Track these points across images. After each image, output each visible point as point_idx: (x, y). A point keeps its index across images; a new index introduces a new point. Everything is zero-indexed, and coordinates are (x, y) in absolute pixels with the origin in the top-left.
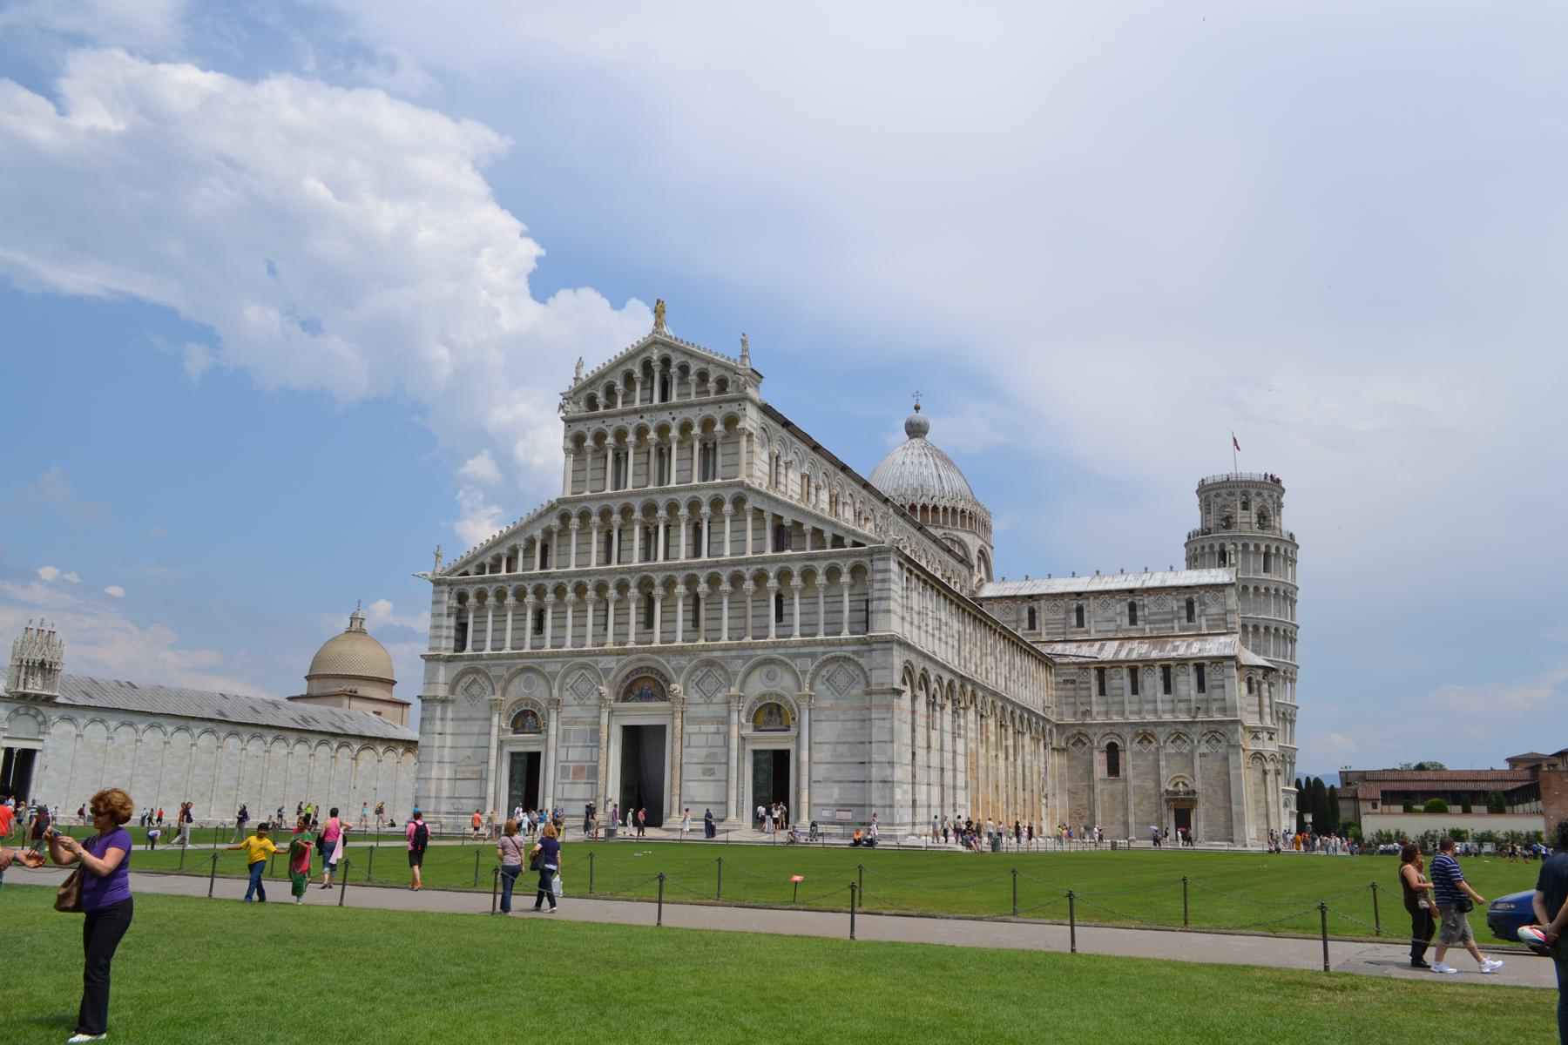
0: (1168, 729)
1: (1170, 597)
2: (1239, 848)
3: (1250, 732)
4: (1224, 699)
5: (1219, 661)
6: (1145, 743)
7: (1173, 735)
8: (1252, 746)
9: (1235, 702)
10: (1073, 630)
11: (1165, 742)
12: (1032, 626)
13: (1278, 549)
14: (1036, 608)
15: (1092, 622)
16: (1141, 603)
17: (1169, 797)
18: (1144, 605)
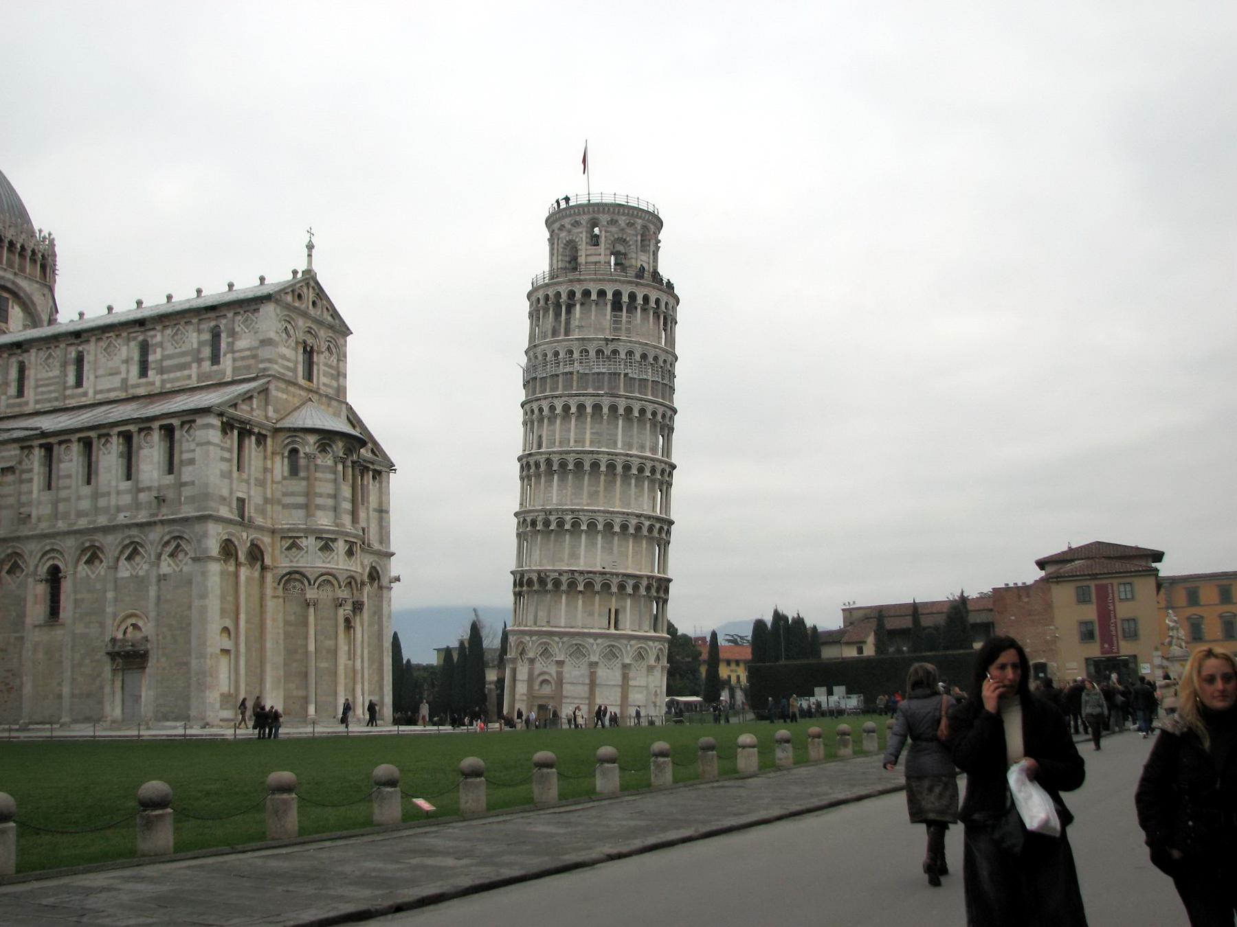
0: (119, 536)
1: (190, 328)
2: (195, 731)
3: (282, 538)
4: (194, 481)
5: (190, 417)
6: (97, 562)
7: (126, 546)
8: (283, 562)
9: (206, 485)
10: (68, 392)
11: (118, 559)
12: (20, 393)
13: (632, 296)
14: (27, 363)
15: (92, 377)
16: (154, 342)
17: (117, 649)
18: (156, 344)
